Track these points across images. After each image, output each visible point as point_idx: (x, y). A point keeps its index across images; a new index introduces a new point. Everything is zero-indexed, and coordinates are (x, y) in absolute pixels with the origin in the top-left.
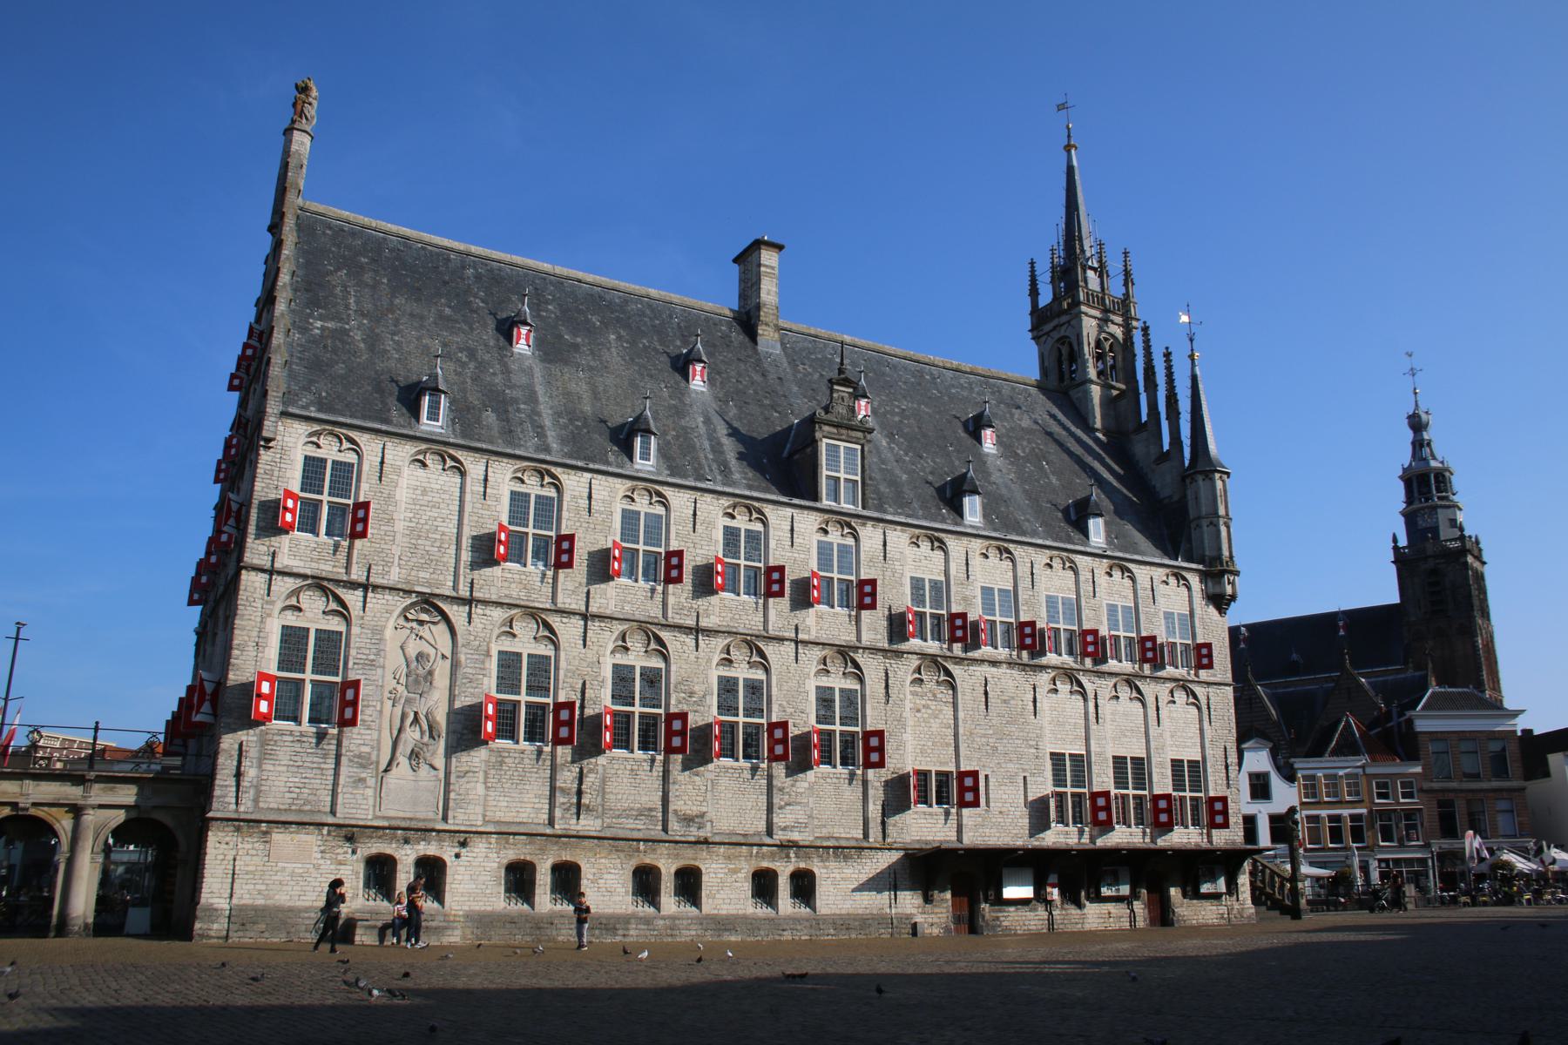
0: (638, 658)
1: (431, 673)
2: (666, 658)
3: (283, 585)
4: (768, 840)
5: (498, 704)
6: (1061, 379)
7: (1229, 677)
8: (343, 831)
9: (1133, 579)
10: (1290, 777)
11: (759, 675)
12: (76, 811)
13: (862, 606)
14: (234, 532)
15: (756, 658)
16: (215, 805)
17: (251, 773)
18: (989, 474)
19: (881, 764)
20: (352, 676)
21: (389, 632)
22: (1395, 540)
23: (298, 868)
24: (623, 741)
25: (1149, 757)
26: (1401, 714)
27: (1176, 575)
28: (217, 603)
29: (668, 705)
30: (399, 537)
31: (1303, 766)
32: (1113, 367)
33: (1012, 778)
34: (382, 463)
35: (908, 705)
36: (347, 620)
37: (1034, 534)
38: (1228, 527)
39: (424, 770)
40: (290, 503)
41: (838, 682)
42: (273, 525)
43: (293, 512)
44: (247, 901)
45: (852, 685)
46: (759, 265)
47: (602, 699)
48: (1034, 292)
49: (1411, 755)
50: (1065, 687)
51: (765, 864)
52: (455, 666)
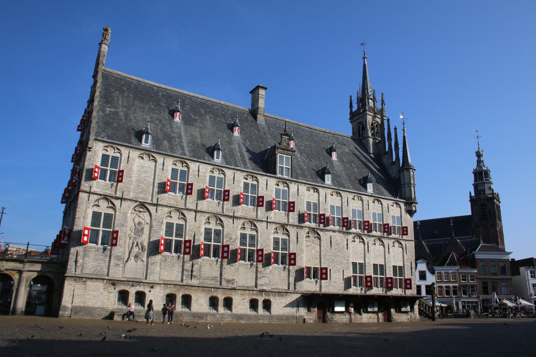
0: (213, 226)
1: (143, 229)
2: (223, 226)
3: (93, 198)
4: (255, 289)
5: (165, 240)
6: (359, 136)
7: (413, 238)
8: (111, 282)
9: (381, 204)
10: (433, 273)
11: (254, 233)
12: (20, 272)
13: (290, 211)
14: (77, 179)
15: (253, 227)
16: (68, 272)
17: (80, 261)
18: (334, 167)
19: (294, 264)
20: (116, 229)
21: (129, 215)
22: (470, 194)
23: (95, 294)
24: (207, 254)
25: (385, 265)
26: (471, 252)
28: (71, 203)
29: (223, 242)
30: (133, 182)
31: (437, 269)
32: (377, 132)
34: (129, 157)
35: (304, 245)
36: (115, 210)
37: (349, 188)
38: (414, 188)
39: (139, 262)
40: (97, 170)
41: (281, 236)
42: (90, 177)
43: (98, 173)
44: (78, 304)
45: (286, 237)
46: (259, 94)
47: (201, 240)
48: (351, 106)
49: (474, 267)
50: (357, 240)
51: (254, 297)
52: (151, 227)
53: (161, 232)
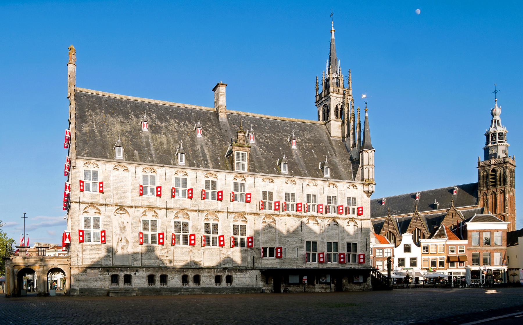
1: (125, 227)
27: (353, 185)
33: (293, 249)
51: (219, 274)
53: (140, 228)
